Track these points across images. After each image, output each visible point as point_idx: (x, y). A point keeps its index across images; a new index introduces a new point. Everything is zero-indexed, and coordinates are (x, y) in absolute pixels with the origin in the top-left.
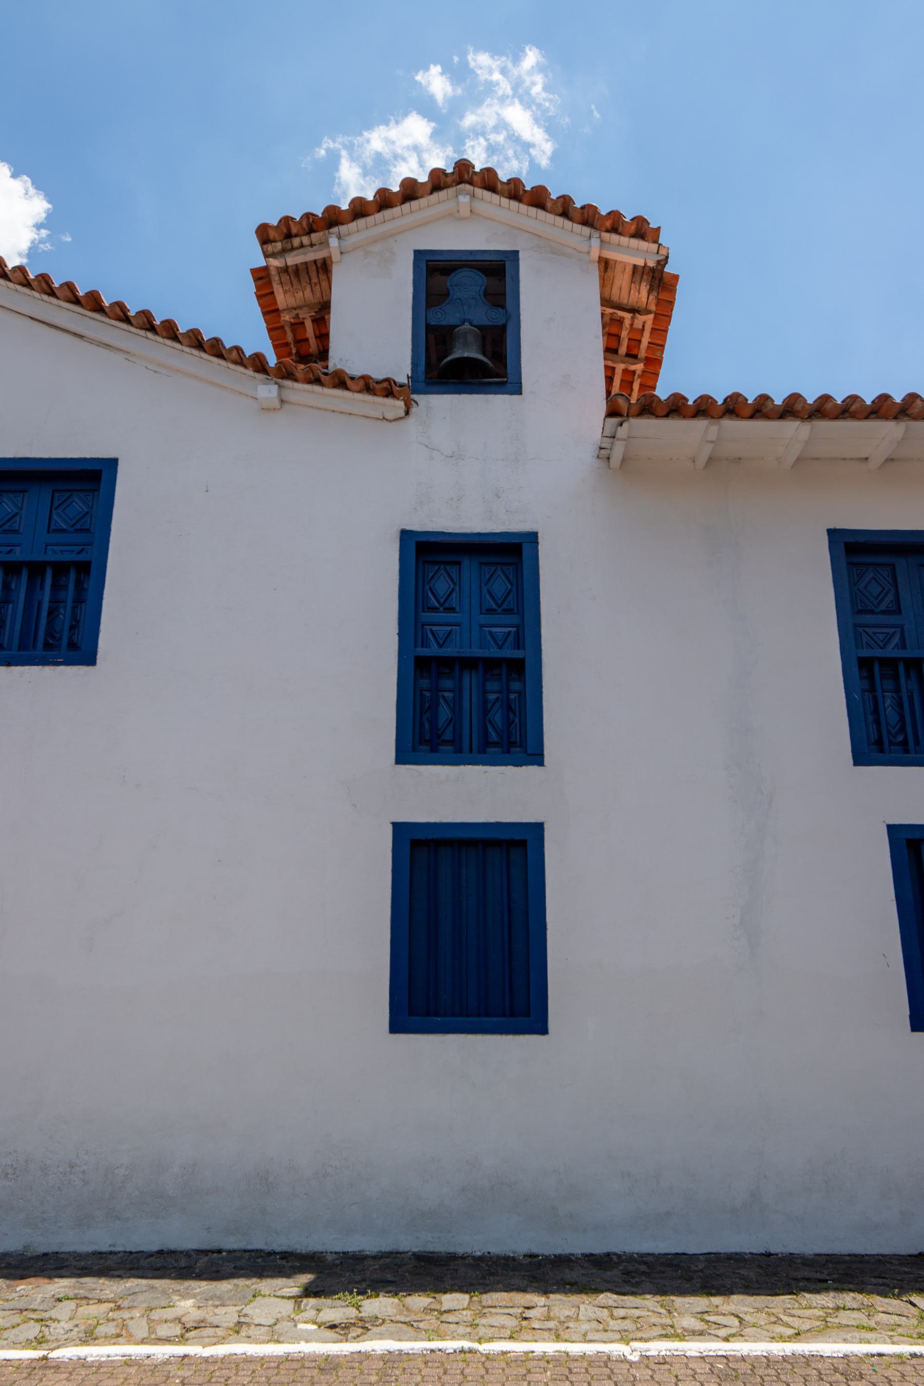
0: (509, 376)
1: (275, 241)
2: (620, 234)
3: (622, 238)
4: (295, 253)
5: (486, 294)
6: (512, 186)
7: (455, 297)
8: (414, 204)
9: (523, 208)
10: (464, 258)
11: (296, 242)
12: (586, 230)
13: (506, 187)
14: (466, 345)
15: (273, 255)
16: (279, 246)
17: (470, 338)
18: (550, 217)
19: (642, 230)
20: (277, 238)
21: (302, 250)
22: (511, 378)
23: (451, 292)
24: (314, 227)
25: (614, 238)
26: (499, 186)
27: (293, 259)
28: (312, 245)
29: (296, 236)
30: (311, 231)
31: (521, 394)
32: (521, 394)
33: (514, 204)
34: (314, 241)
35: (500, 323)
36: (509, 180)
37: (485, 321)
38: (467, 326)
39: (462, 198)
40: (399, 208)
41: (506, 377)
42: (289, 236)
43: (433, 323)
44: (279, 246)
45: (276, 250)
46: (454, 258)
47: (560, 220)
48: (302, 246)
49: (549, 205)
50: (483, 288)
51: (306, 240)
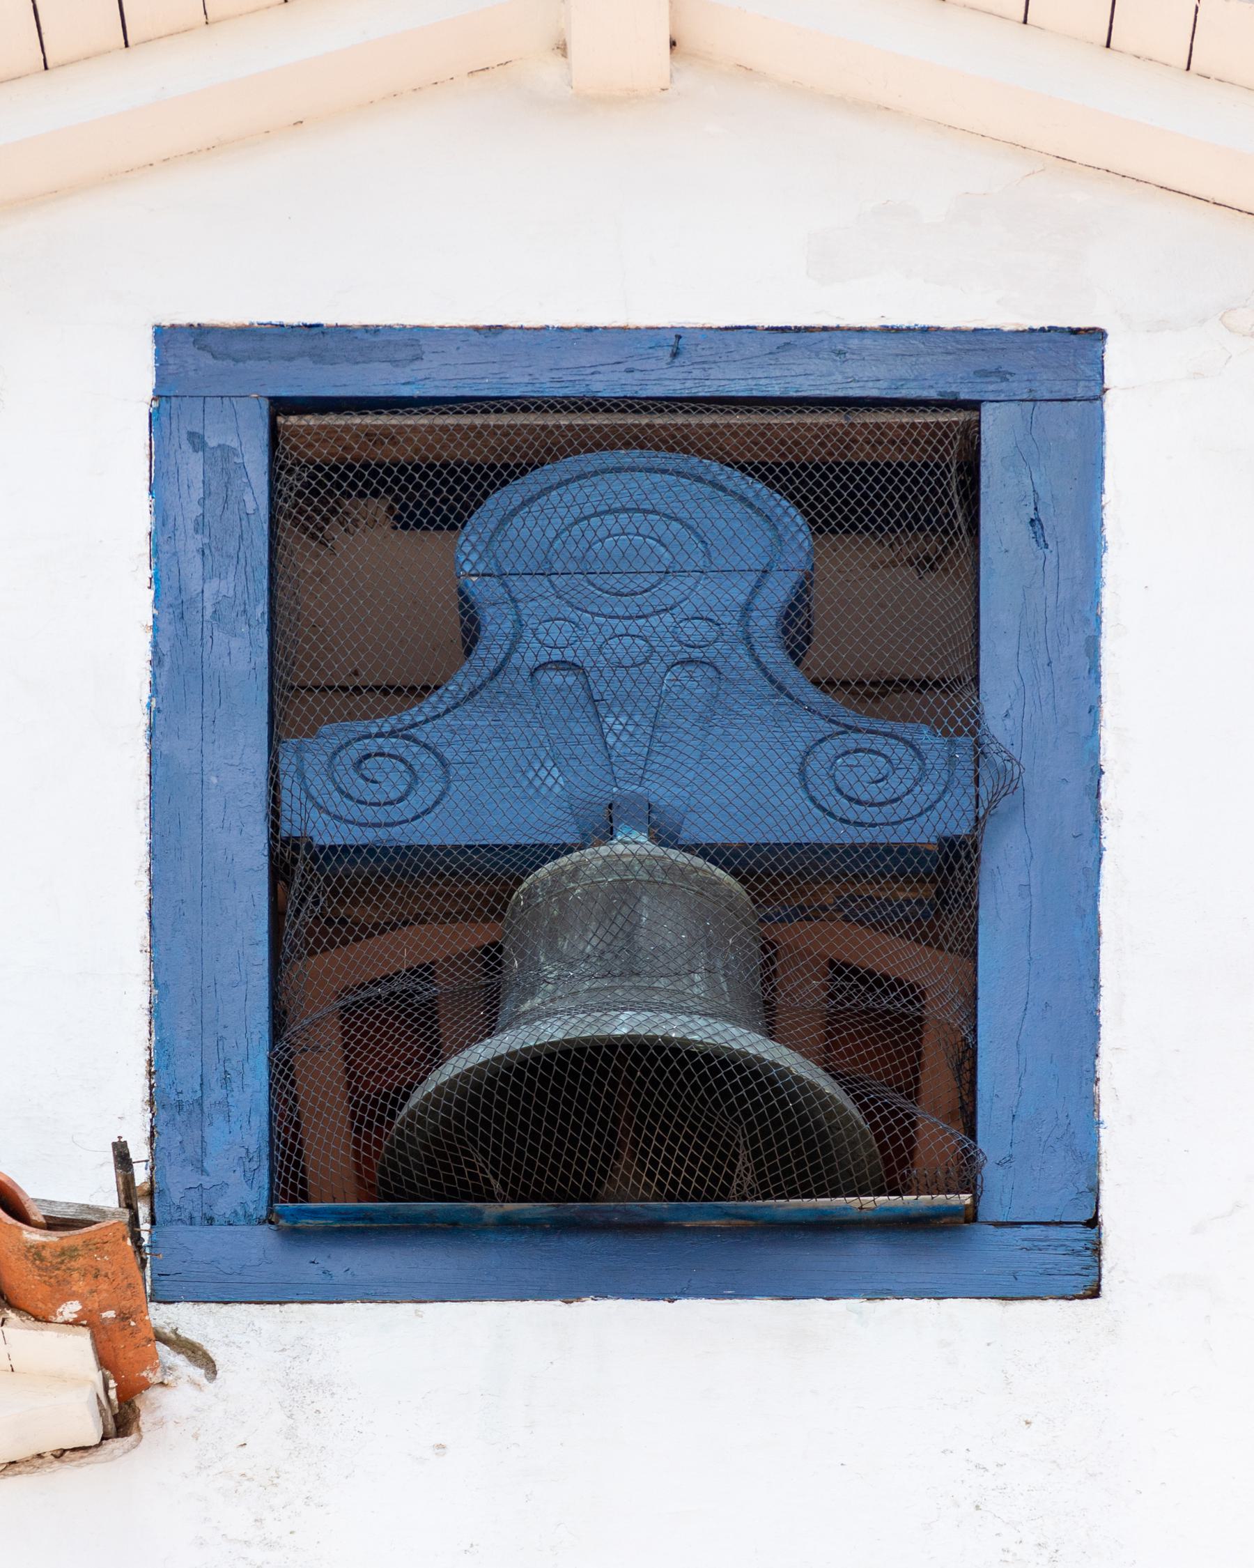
0: (991, 1175)
5: (797, 630)
7: (529, 655)
10: (605, 385)
14: (625, 967)
17: (663, 926)
22: (1002, 1191)
23: (496, 624)
31: (1095, 1293)
32: (1095, 1293)
35: (924, 833)
37: (781, 814)
38: (632, 843)
41: (969, 1184)
43: (326, 833)
46: (517, 384)
50: (779, 591)
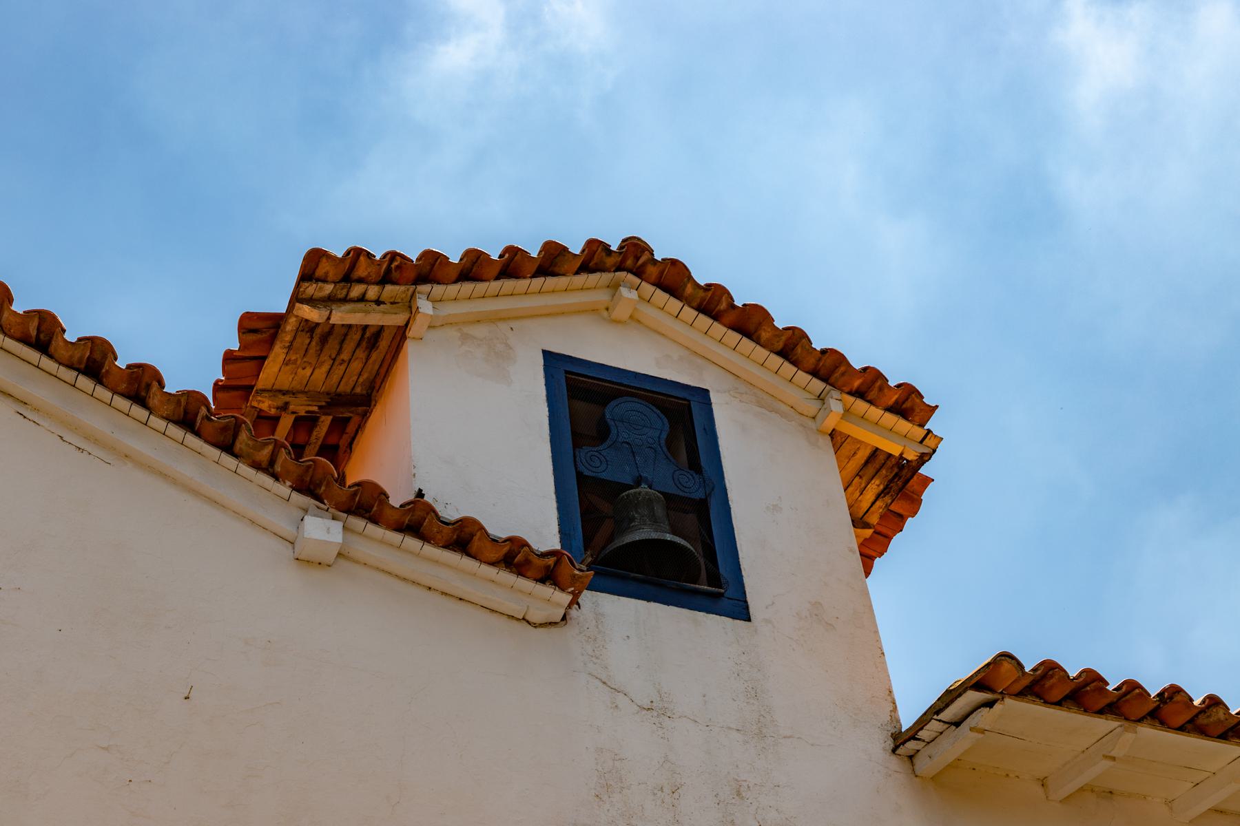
1: (325, 281)
2: (871, 402)
3: (873, 408)
4: (348, 307)
6: (710, 294)
8: (551, 282)
9: (719, 329)
11: (357, 290)
12: (818, 385)
13: (701, 294)
15: (311, 301)
16: (328, 288)
18: (761, 353)
19: (908, 404)
20: (331, 277)
21: (361, 305)
24: (395, 275)
25: (861, 406)
26: (689, 289)
27: (341, 316)
28: (378, 302)
29: (361, 281)
30: (386, 279)
33: (704, 321)
34: (384, 297)
36: (709, 286)
39: (631, 292)
40: (527, 281)
42: (348, 278)
44: (328, 288)
45: (319, 295)
47: (776, 360)
48: (362, 299)
49: (765, 335)
51: (373, 291)
